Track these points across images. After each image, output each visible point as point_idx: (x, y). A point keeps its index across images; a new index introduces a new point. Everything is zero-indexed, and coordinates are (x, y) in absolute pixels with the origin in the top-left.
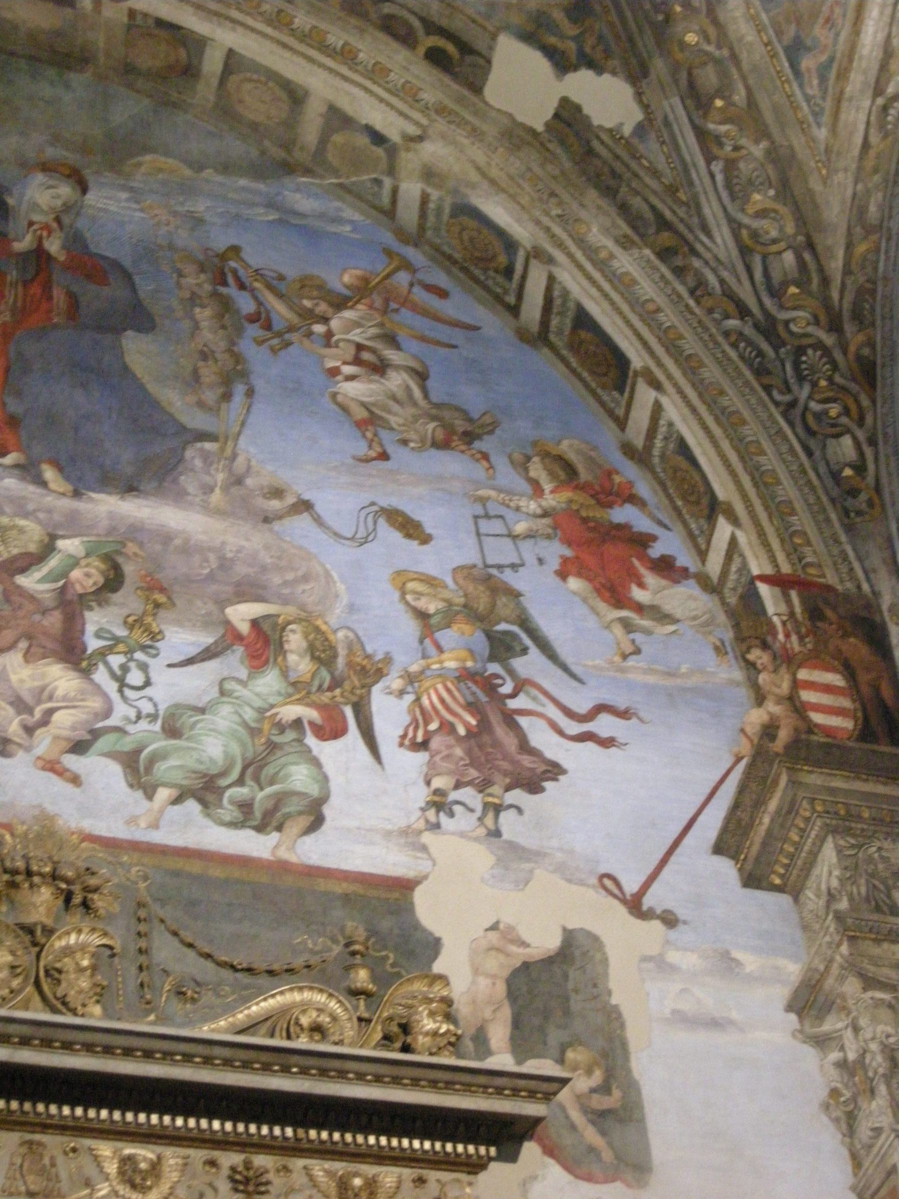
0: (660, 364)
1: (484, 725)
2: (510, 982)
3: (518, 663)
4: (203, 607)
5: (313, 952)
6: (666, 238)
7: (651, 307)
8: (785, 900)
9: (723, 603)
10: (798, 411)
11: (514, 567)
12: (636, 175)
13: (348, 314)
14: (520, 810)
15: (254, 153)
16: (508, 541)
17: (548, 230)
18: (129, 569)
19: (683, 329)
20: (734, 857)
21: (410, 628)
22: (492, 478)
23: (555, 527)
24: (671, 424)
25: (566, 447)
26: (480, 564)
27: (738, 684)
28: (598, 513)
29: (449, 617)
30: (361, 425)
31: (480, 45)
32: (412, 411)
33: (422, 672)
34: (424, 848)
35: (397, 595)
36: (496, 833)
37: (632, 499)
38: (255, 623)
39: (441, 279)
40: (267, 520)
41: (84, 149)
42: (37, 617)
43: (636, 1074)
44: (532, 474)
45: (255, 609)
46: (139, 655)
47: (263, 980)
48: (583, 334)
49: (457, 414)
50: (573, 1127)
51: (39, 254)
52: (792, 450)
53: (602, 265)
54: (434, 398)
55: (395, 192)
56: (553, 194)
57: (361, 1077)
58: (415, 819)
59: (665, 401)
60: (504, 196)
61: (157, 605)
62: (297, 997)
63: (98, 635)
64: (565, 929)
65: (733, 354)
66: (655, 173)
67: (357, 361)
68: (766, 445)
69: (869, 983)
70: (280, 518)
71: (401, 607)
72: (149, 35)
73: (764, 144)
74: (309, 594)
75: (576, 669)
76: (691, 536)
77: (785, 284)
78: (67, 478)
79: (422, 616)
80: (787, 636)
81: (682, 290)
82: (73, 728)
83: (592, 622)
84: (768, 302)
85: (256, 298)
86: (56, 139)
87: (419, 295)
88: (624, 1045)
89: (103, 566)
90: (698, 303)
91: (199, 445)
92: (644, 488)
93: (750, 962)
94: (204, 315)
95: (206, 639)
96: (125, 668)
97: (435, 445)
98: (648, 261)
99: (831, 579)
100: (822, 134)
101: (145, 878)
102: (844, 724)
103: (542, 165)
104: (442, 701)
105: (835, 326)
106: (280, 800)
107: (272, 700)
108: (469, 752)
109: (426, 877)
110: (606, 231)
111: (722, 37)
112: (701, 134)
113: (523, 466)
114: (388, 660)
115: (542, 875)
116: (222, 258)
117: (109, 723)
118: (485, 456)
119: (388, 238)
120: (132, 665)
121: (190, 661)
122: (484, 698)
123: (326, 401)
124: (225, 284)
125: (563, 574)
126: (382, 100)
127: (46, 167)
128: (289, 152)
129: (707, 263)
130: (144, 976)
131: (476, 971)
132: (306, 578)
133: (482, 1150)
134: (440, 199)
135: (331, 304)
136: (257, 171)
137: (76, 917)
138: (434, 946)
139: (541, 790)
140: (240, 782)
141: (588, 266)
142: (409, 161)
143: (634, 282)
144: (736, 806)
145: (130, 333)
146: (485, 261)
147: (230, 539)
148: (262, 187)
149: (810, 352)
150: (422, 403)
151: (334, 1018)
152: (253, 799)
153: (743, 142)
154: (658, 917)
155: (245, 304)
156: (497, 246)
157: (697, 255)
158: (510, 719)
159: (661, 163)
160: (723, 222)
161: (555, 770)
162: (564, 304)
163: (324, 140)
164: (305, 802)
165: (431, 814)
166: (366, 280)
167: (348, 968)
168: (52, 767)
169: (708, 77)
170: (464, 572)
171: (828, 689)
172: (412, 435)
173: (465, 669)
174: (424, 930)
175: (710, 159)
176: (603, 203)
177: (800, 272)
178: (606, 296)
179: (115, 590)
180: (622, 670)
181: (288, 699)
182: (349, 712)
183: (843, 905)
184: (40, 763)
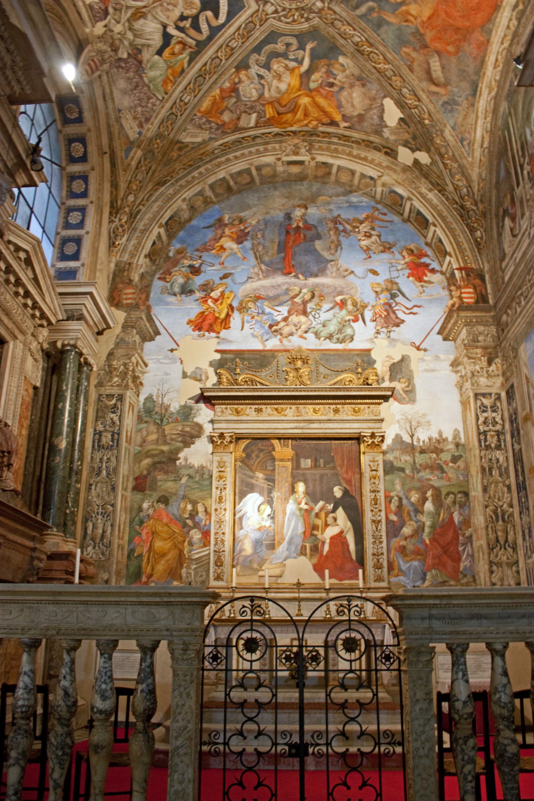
1: (388, 314)
3: (397, 299)
4: (331, 299)
6: (440, 188)
8: (452, 343)
13: (364, 225)
17: (411, 192)
18: (316, 293)
19: (444, 210)
21: (374, 295)
25: (412, 246)
28: (418, 261)
29: (382, 291)
30: (365, 251)
31: (395, 149)
37: (427, 256)
39: (385, 211)
41: (307, 200)
45: (340, 297)
51: (298, 227)
53: (424, 197)
58: (373, 337)
59: (437, 229)
67: (365, 236)
68: (461, 236)
69: (469, 358)
74: (352, 292)
79: (376, 292)
83: (414, 287)
86: (301, 199)
87: (381, 217)
92: (429, 252)
93: (442, 357)
94: (332, 233)
95: (331, 305)
97: (382, 252)
99: (473, 266)
100: (470, 159)
102: (472, 300)
105: (476, 204)
106: (345, 337)
110: (426, 188)
111: (445, 140)
112: (443, 163)
113: (401, 253)
115: (398, 345)
119: (373, 203)
125: (408, 277)
127: (299, 206)
131: (383, 366)
136: (345, 194)
138: (375, 362)
142: (379, 183)
144: (444, 323)
146: (395, 204)
148: (345, 198)
155: (341, 228)
158: (394, 312)
159: (436, 171)
161: (403, 321)
163: (359, 182)
168: (301, 337)
169: (443, 150)
170: (387, 281)
171: (469, 293)
175: (446, 169)
176: (425, 181)
181: (347, 315)
183: (466, 342)
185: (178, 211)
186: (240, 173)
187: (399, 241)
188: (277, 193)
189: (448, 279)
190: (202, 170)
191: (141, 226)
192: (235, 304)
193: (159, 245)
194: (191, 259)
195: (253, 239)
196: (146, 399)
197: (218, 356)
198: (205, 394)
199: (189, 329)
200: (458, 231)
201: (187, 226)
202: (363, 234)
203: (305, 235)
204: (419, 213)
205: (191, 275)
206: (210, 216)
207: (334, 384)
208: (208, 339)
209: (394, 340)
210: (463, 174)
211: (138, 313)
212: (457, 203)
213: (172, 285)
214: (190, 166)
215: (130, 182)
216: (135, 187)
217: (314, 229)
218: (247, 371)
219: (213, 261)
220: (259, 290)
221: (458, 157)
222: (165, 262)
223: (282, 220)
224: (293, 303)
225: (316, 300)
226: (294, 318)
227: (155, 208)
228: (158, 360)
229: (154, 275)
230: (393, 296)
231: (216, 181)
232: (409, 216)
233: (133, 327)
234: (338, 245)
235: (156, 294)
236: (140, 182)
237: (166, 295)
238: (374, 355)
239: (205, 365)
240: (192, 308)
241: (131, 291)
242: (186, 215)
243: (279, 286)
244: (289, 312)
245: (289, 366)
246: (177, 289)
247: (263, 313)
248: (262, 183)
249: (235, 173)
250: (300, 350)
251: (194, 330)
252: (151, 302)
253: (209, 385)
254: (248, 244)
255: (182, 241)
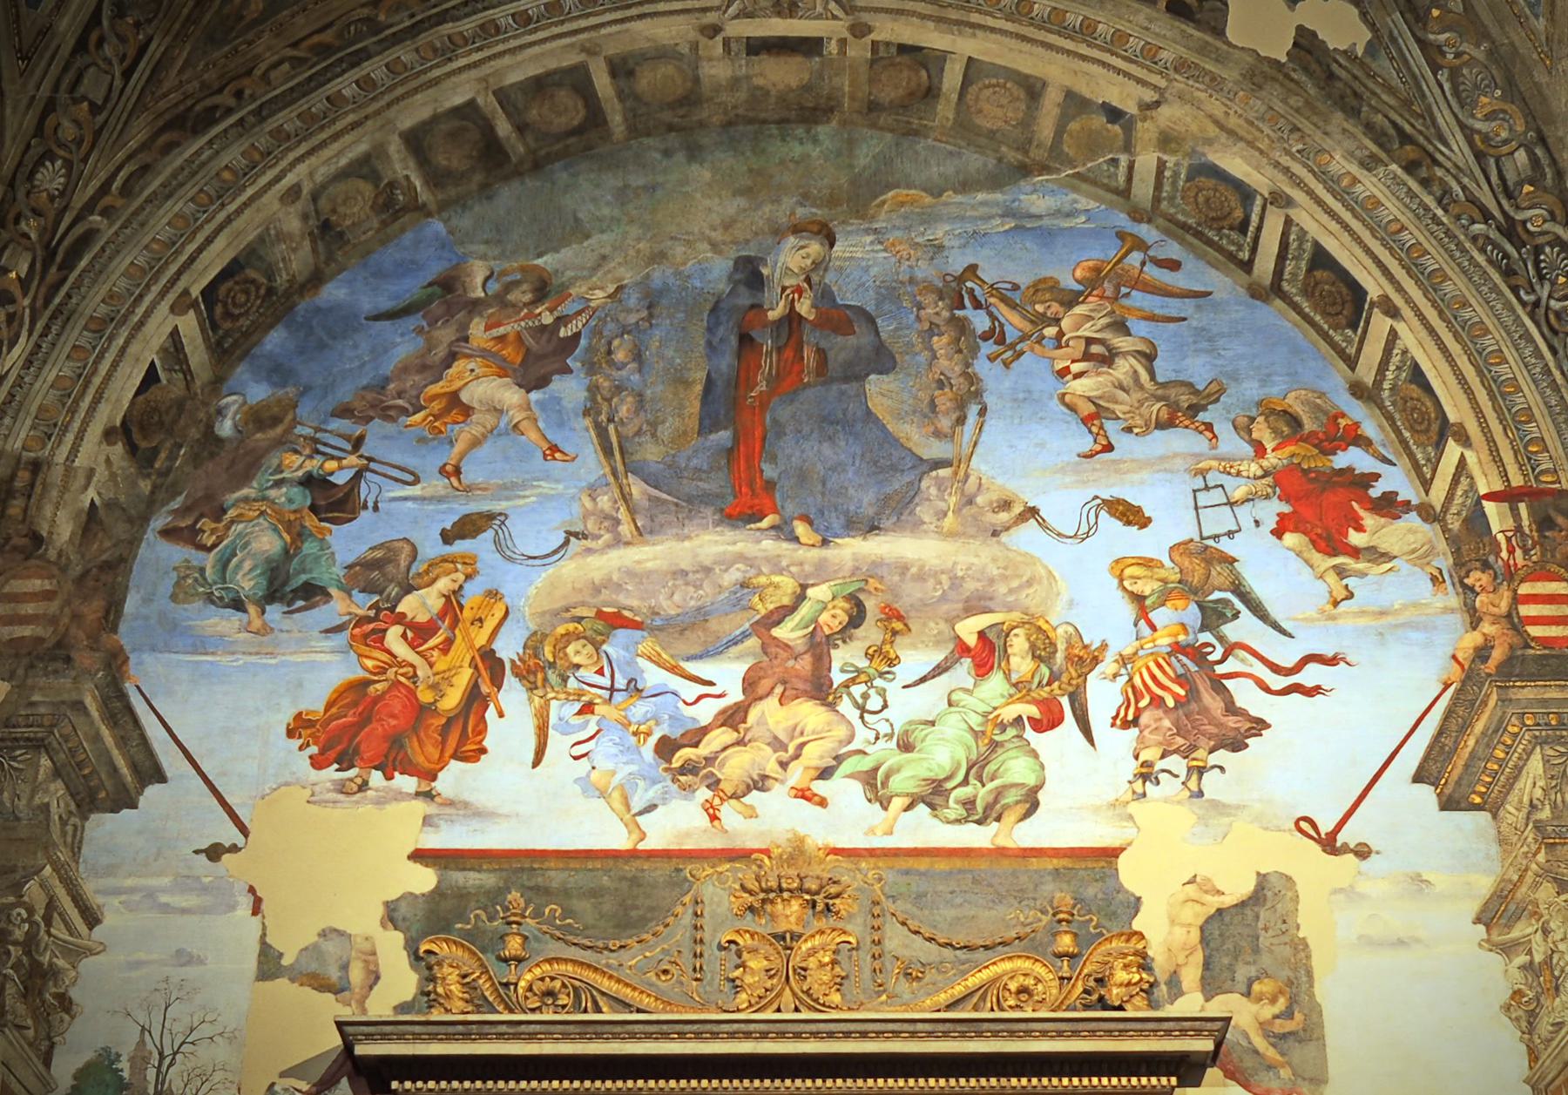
0: (1400, 289)
1: (1193, 694)
2: (1202, 929)
3: (1231, 631)
4: (935, 627)
5: (1024, 925)
6: (1410, 152)
7: (1394, 227)
9: (1445, 530)
10: (1542, 310)
11: (1230, 534)
12: (1374, 93)
13: (1079, 310)
14: (1222, 769)
15: (992, 162)
16: (1227, 508)
17: (1286, 170)
18: (870, 604)
20: (1435, 784)
21: (1128, 611)
22: (1214, 447)
23: (1277, 483)
24: (1405, 352)
26: (1197, 539)
27: (1453, 611)
28: (1319, 463)
29: (1164, 599)
30: (1087, 421)
32: (1139, 395)
33: (1135, 653)
34: (1131, 817)
35: (1116, 582)
36: (1200, 794)
38: (982, 635)
39: (1173, 250)
40: (995, 534)
41: (832, 201)
42: (791, 663)
43: (1319, 999)
44: (1255, 435)
46: (878, 682)
47: (980, 955)
48: (1318, 274)
49: (1183, 389)
50: (1256, 1052)
52: (1537, 353)
54: (1160, 379)
55: (1131, 167)
56: (1295, 129)
57: (1044, 1034)
58: (1123, 791)
59: (1401, 328)
60: (1241, 145)
61: (895, 633)
62: (1007, 966)
63: (843, 671)
64: (1258, 874)
65: (1481, 259)
66: (1391, 90)
67: (1087, 357)
70: (1007, 529)
71: (1120, 593)
72: (893, 65)
73: (1485, 46)
74: (1031, 599)
75: (1284, 625)
76: (1417, 467)
77: (1520, 184)
78: (817, 531)
80: (1511, 551)
81: (1429, 200)
82: (822, 757)
84: (1504, 202)
85: (990, 314)
86: (805, 198)
87: (1152, 272)
88: (1310, 974)
89: (847, 606)
90: (1446, 211)
91: (934, 473)
92: (1370, 429)
95: (938, 657)
96: (865, 696)
97: (1161, 425)
98: (1395, 177)
101: (880, 880)
103: (1284, 101)
104: (1153, 677)
106: (999, 793)
107: (995, 704)
108: (1176, 724)
109: (1129, 844)
110: (1350, 155)
113: (1244, 429)
114: (1104, 646)
116: (960, 279)
117: (851, 747)
118: (1209, 427)
119: (1122, 220)
120: (872, 692)
121: (923, 680)
122: (1193, 668)
123: (1055, 403)
124: (963, 307)
125: (1278, 533)
126: (1119, 71)
127: (797, 230)
128: (1026, 152)
129: (1448, 171)
130: (877, 964)
131: (1173, 922)
132: (1029, 583)
133: (1164, 1080)
134: (1177, 164)
135: (1062, 304)
136: (994, 182)
137: (822, 923)
139: (1247, 746)
140: (965, 782)
141: (1329, 200)
142: (1146, 131)
143: (1379, 203)
145: (872, 377)
147: (961, 558)
148: (998, 196)
149: (1548, 250)
150: (1148, 385)
151: (1038, 980)
152: (975, 796)
153: (1465, 47)
154: (1352, 851)
155: (981, 322)
156: (1234, 200)
157: (1440, 165)
160: (1457, 129)
161: (1259, 726)
162: (1300, 247)
163: (1060, 131)
164: (1023, 792)
165: (1138, 786)
166: (1098, 270)
167: (1055, 934)
168: (804, 794)
172: (1139, 422)
173: (1177, 643)
174: (1127, 892)
175: (1435, 69)
177: (1533, 169)
178: (1346, 227)
179: (857, 626)
180: (1333, 618)
181: (1011, 700)
182: (1065, 701)
184: (793, 792)
185: (261, 239)
186: (539, 86)
187: (1235, 377)
188: (702, 173)
189: (1453, 541)
190: (374, 68)
191: (94, 303)
192: (508, 648)
193: (171, 385)
194: (315, 447)
195: (591, 368)
196: (82, 1075)
197: (424, 880)
198: (360, 1050)
199: (297, 759)
200: (1497, 333)
201: (302, 306)
202: (1078, 348)
203: (821, 353)
204: (1321, 258)
205: (311, 521)
206: (406, 268)
207: (951, 1006)
208: (380, 802)
209: (1218, 807)
210: (1512, 91)
211: (65, 682)
212: (1486, 216)
213: (224, 564)
214: (324, 50)
215: (50, 107)
216: (68, 131)
217: (860, 327)
218: (555, 949)
219: (411, 462)
220: (619, 587)
221: (1486, 17)
222: (196, 460)
223: (723, 287)
224: (771, 646)
225: (870, 633)
226: (770, 714)
227: (160, 225)
228: (151, 894)
229: (145, 519)
230: (1214, 616)
231: (435, 119)
232: (1278, 272)
233: (38, 745)
234: (971, 395)
235: (148, 600)
236: (95, 109)
237: (199, 604)
238: (1130, 873)
239: (364, 920)
240: (313, 665)
241: (37, 584)
242: (297, 260)
243: (707, 570)
244: (749, 683)
245: (749, 922)
246: (247, 582)
247: (635, 689)
248: (636, 130)
249: (521, 86)
250: (797, 852)
251: (317, 763)
252: (126, 635)
253: (380, 1006)
254: (570, 389)
255: (278, 372)
